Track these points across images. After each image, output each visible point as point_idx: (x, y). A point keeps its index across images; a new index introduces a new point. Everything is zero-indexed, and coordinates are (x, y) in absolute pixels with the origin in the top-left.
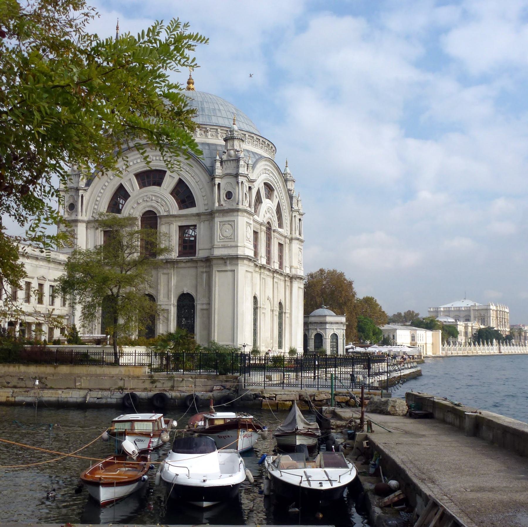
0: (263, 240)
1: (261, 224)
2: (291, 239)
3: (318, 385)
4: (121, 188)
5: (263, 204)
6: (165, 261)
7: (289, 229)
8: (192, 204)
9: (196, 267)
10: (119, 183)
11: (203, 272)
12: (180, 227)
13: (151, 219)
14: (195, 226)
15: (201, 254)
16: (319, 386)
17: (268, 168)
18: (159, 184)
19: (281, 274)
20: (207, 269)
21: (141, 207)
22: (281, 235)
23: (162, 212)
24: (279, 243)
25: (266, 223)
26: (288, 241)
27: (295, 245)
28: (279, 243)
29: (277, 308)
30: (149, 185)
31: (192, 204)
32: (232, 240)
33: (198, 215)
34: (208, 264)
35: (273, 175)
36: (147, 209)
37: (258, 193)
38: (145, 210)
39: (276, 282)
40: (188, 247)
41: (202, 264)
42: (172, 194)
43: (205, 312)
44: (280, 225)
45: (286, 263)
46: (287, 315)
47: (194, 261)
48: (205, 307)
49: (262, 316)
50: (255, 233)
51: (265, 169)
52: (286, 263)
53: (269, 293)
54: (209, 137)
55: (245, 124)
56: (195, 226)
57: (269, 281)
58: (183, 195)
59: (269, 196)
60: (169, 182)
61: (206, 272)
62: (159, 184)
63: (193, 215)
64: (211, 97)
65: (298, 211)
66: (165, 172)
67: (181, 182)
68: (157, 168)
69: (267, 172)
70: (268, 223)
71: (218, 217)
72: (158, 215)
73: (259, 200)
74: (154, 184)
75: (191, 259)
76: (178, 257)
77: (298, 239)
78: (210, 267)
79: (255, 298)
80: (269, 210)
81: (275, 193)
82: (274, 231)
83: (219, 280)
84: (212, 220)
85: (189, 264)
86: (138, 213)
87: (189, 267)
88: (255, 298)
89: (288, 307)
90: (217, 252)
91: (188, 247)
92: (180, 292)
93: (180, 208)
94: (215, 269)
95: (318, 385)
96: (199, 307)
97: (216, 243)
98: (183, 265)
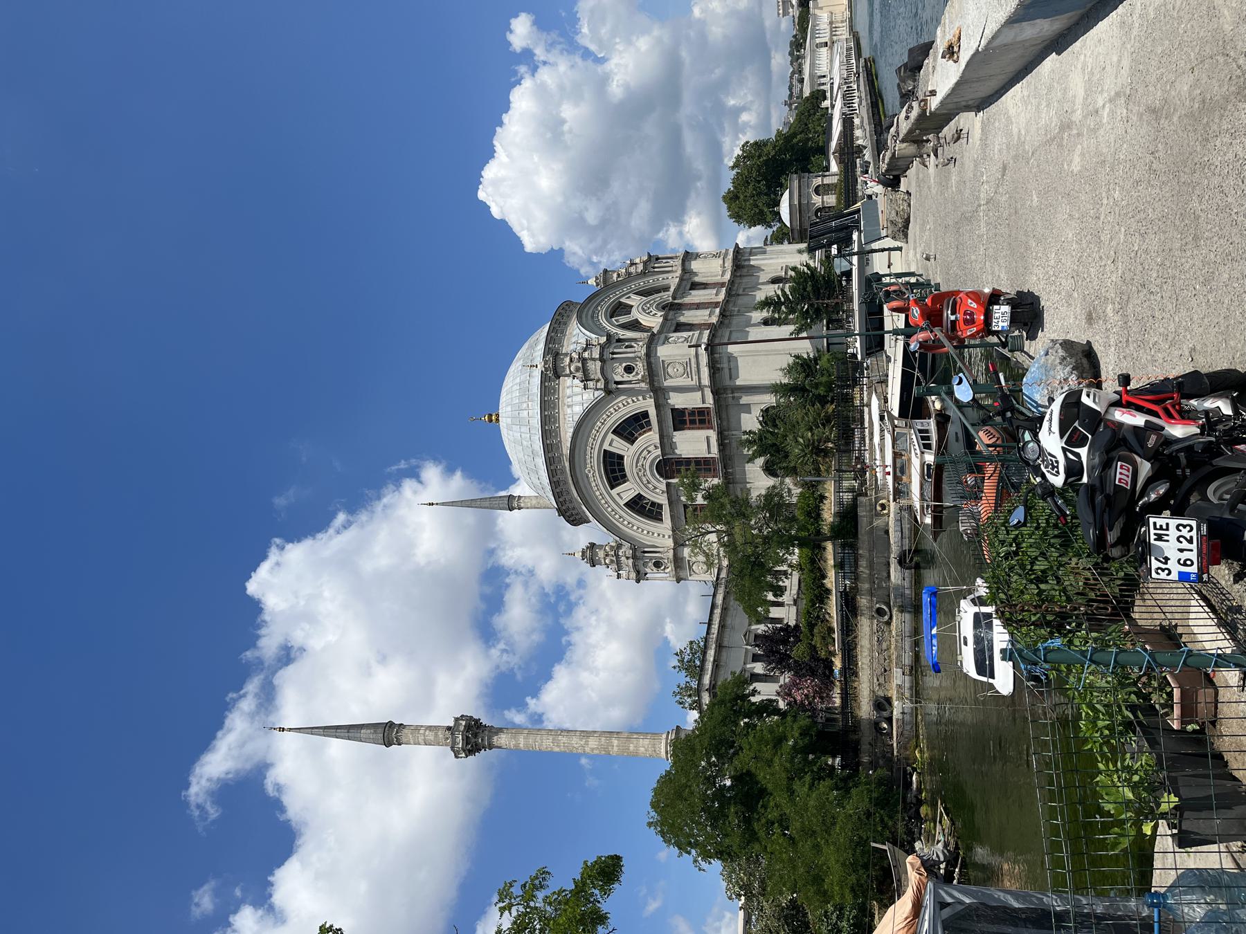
7: (670, 276)
8: (645, 415)
13: (668, 466)
18: (621, 457)
22: (679, 285)
27: (695, 265)
31: (645, 415)
37: (624, 326)
44: (666, 289)
50: (680, 327)
52: (718, 279)
58: (631, 428)
59: (627, 309)
60: (618, 446)
62: (621, 457)
65: (645, 263)
70: (663, 308)
77: (683, 261)
78: (725, 389)
81: (623, 300)
82: (674, 298)
85: (724, 416)
94: (728, 383)
97: (693, 383)
98: (725, 423)
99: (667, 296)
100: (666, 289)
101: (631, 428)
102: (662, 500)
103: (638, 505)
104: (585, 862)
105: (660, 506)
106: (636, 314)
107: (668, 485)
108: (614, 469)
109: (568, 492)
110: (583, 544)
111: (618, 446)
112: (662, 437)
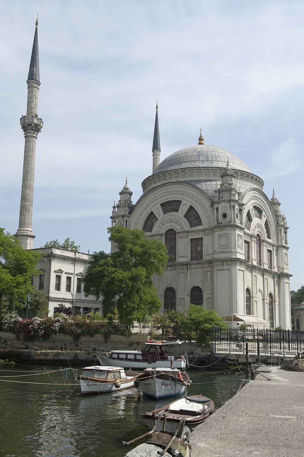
0: (253, 249)
1: (251, 236)
2: (278, 247)
3: (284, 352)
4: (152, 213)
5: (253, 222)
6: (181, 264)
8: (200, 223)
9: (203, 268)
10: (150, 211)
11: (207, 271)
12: (191, 239)
13: (171, 235)
14: (202, 238)
15: (206, 258)
16: (285, 353)
17: (257, 195)
18: (177, 211)
19: (270, 272)
20: (211, 269)
21: (164, 227)
23: (178, 229)
24: (268, 250)
25: (256, 235)
26: (275, 248)
28: (268, 250)
29: (267, 300)
30: (170, 211)
31: (200, 223)
32: (228, 248)
33: (204, 230)
34: (211, 265)
35: (261, 200)
36: (169, 228)
37: (249, 214)
38: (167, 229)
39: (266, 278)
40: (197, 253)
41: (207, 265)
42: (185, 216)
43: (210, 300)
45: (275, 264)
46: (277, 303)
47: (201, 263)
48: (210, 296)
49: (255, 303)
51: (254, 196)
53: (260, 286)
54: (211, 175)
55: (238, 165)
56: (202, 238)
57: (260, 278)
61: (210, 271)
62: (177, 211)
63: (200, 231)
64: (214, 148)
66: (181, 202)
67: (191, 208)
68: (175, 199)
69: (256, 198)
71: (218, 231)
72: (176, 232)
73: (249, 218)
74: (173, 211)
75: (199, 262)
76: (190, 261)
78: (213, 267)
79: (248, 290)
80: (258, 225)
82: (263, 241)
83: (220, 276)
84: (213, 234)
85: (198, 266)
86: (163, 231)
87: (198, 268)
88: (248, 290)
89: (277, 297)
90: (217, 256)
91: (197, 253)
92: (192, 286)
93: (192, 227)
94: (216, 268)
95: (284, 352)
96: (205, 297)
99: (264, 237)
100: (269, 237)
101: (193, 216)
102: (155, 231)
103: (151, 218)
104: (4, 229)
105: (151, 231)
106: (256, 220)
107: (162, 235)
108: (170, 206)
109: (159, 181)
110: (131, 189)
111: (183, 209)
112: (188, 232)
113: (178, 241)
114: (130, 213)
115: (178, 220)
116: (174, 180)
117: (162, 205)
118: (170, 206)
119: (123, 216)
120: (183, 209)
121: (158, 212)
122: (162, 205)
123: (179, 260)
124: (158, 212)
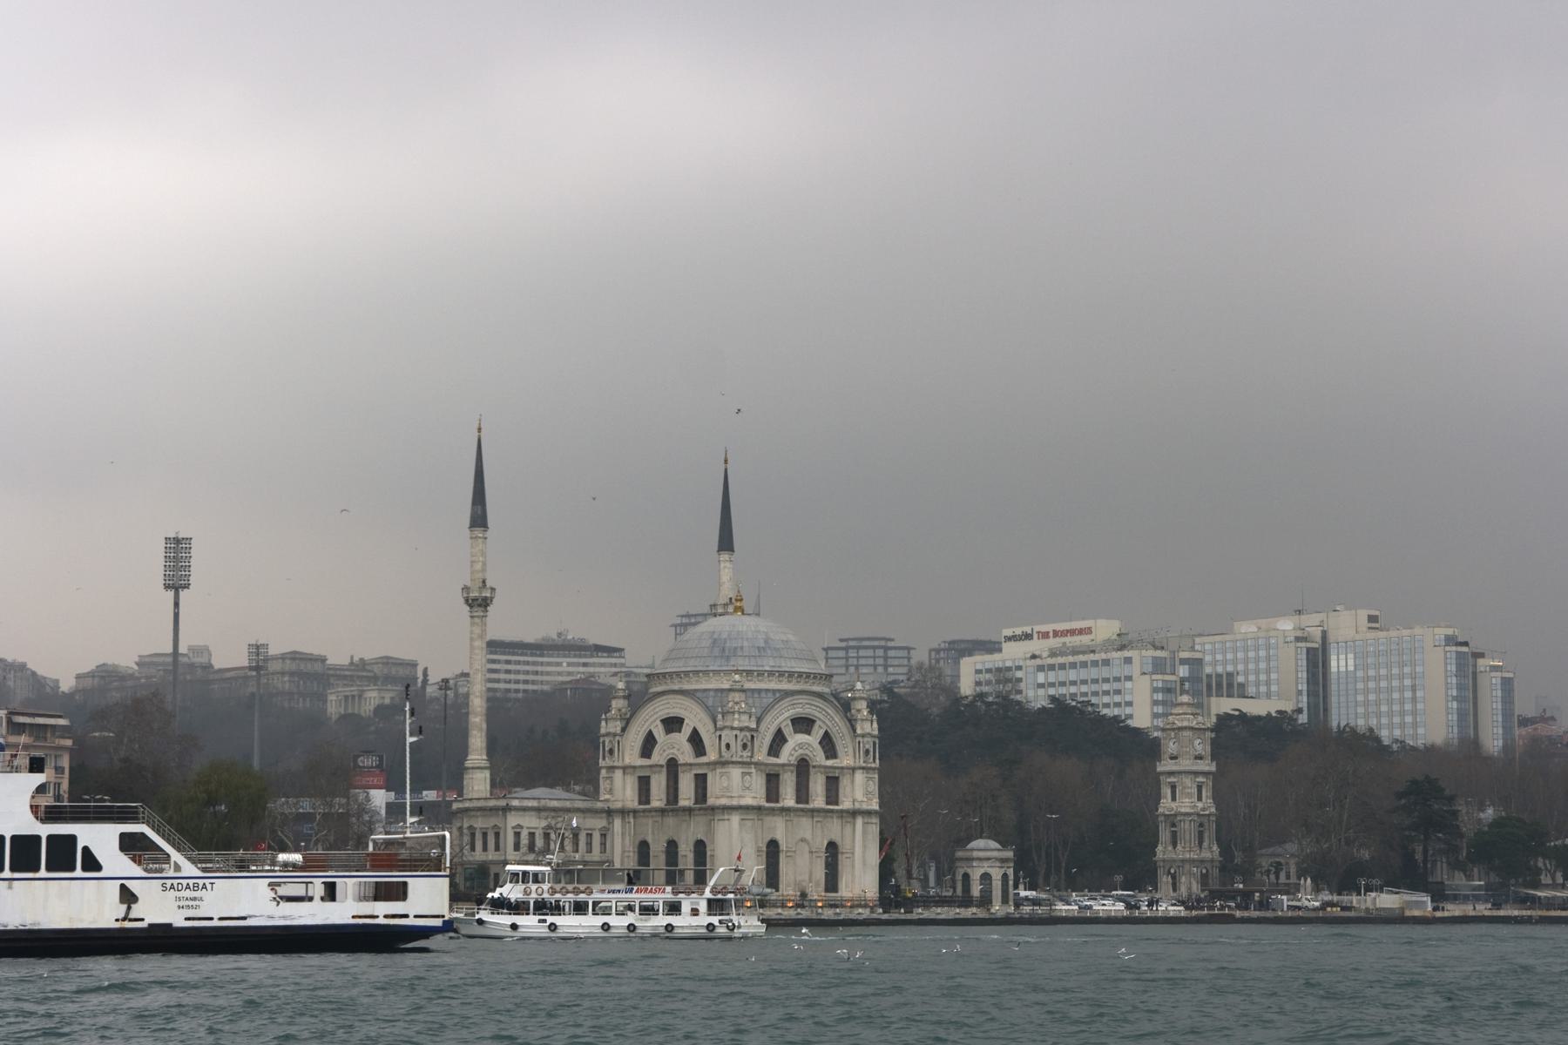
15: (711, 801)
33: (708, 764)
58: (696, 740)
101: (696, 740)
108: (673, 724)
111: (687, 731)
113: (681, 776)
114: (624, 730)
115: (676, 746)
116: (676, 687)
117: (664, 721)
118: (673, 724)
119: (615, 735)
120: (687, 731)
121: (659, 732)
122: (664, 721)
123: (683, 803)
124: (659, 732)
